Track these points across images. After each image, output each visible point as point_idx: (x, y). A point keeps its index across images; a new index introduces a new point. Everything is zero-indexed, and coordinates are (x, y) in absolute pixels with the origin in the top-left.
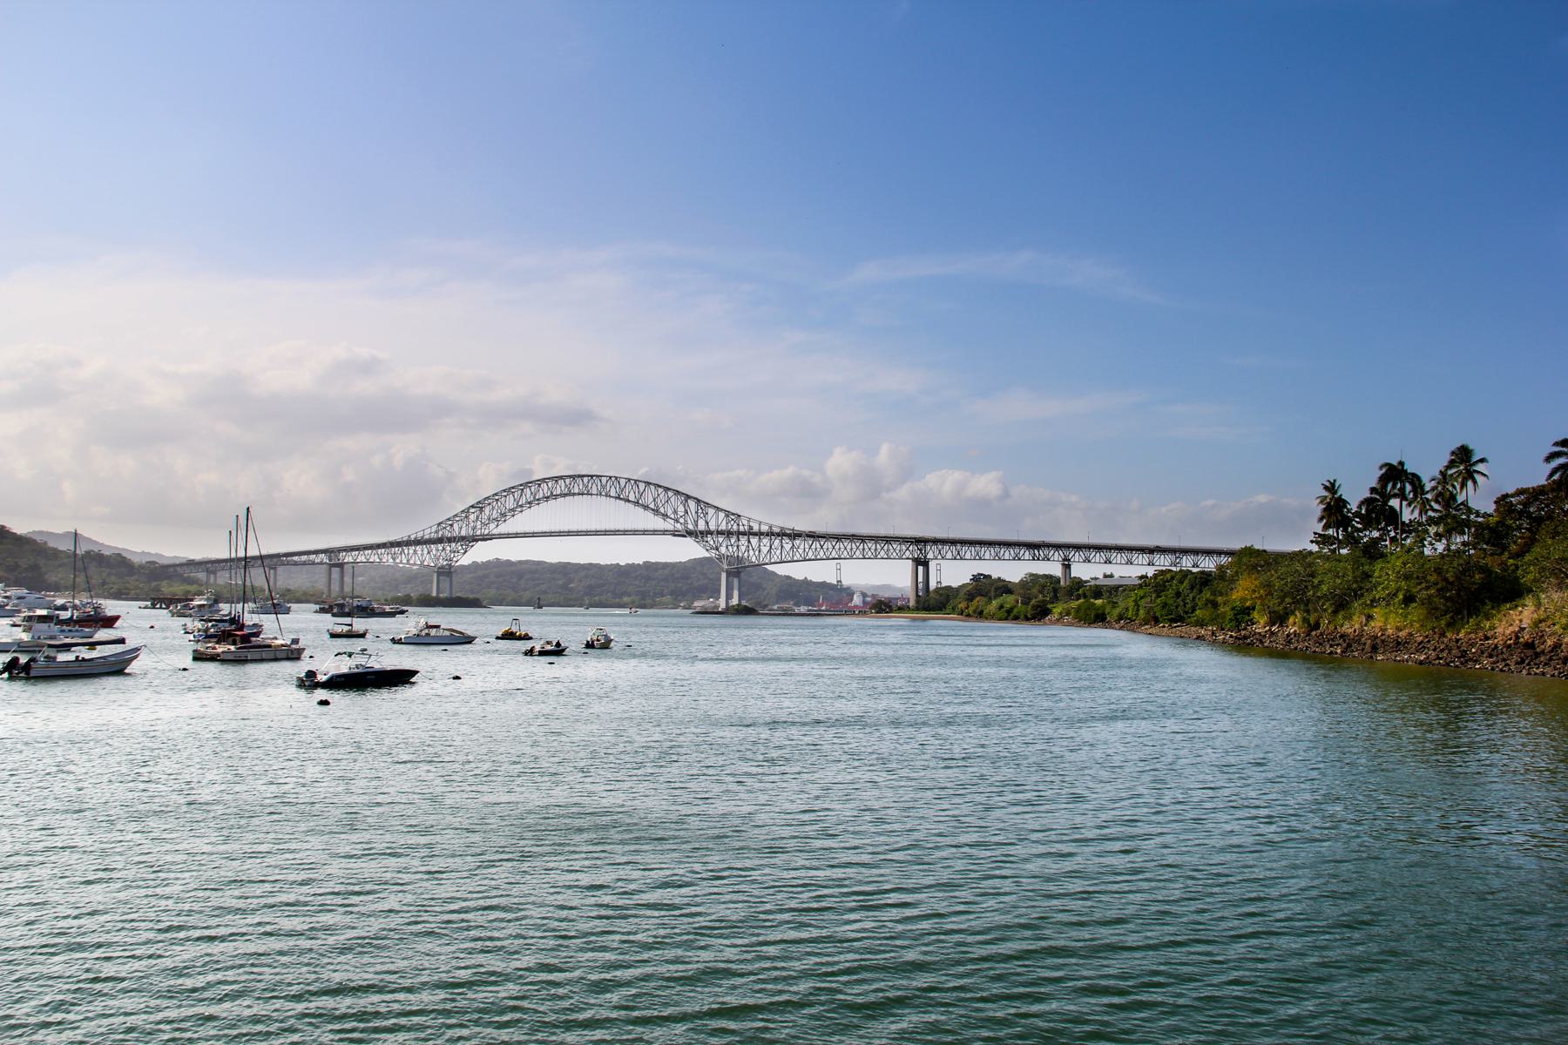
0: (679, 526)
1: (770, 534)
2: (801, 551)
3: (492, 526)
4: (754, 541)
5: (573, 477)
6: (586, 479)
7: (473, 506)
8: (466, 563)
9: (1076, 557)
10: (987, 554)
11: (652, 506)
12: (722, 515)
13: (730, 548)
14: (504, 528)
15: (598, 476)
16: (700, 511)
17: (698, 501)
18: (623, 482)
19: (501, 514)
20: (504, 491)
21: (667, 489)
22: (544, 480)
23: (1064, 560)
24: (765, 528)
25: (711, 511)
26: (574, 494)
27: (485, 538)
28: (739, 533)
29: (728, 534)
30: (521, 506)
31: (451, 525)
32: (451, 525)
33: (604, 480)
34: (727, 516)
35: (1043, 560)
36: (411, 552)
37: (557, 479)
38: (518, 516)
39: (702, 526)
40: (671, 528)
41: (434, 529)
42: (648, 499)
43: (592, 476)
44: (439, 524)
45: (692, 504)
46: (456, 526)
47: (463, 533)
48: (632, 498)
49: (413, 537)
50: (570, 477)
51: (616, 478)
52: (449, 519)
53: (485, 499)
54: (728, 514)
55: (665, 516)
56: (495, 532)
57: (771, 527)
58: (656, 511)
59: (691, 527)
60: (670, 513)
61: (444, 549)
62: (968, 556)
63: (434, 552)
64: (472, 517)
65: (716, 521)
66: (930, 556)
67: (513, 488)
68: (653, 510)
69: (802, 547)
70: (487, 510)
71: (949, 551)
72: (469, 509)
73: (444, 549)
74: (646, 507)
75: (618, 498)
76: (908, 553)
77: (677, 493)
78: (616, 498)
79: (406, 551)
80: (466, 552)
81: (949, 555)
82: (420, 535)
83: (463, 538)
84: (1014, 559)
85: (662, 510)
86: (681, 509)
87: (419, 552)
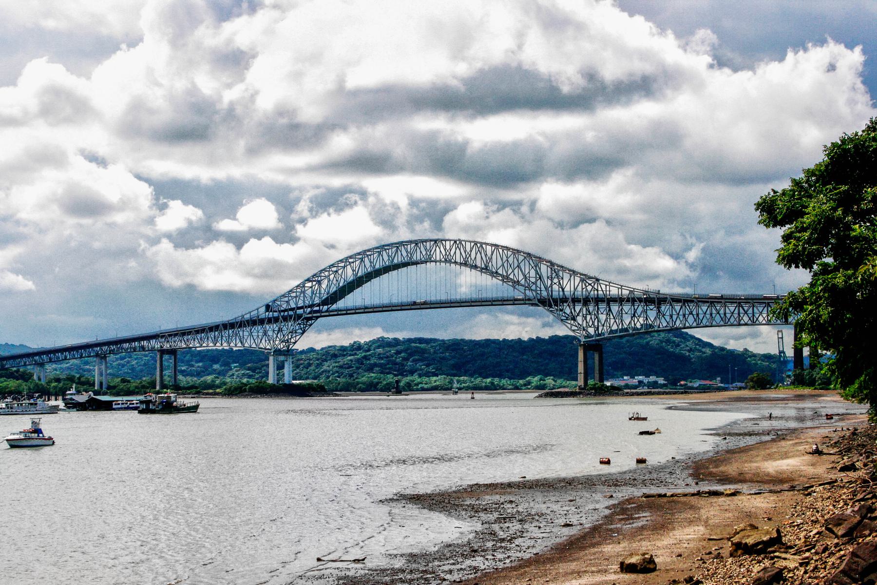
2: (668, 318)
7: (308, 280)
12: (577, 280)
13: (588, 317)
16: (554, 275)
24: (626, 292)
28: (598, 300)
29: (586, 301)
34: (582, 280)
36: (246, 333)
43: (436, 241)
49: (247, 317)
53: (321, 271)
54: (585, 278)
61: (280, 330)
65: (570, 286)
69: (668, 314)
72: (303, 284)
78: (461, 264)
79: (241, 333)
80: (304, 332)
86: (533, 273)
87: (255, 334)
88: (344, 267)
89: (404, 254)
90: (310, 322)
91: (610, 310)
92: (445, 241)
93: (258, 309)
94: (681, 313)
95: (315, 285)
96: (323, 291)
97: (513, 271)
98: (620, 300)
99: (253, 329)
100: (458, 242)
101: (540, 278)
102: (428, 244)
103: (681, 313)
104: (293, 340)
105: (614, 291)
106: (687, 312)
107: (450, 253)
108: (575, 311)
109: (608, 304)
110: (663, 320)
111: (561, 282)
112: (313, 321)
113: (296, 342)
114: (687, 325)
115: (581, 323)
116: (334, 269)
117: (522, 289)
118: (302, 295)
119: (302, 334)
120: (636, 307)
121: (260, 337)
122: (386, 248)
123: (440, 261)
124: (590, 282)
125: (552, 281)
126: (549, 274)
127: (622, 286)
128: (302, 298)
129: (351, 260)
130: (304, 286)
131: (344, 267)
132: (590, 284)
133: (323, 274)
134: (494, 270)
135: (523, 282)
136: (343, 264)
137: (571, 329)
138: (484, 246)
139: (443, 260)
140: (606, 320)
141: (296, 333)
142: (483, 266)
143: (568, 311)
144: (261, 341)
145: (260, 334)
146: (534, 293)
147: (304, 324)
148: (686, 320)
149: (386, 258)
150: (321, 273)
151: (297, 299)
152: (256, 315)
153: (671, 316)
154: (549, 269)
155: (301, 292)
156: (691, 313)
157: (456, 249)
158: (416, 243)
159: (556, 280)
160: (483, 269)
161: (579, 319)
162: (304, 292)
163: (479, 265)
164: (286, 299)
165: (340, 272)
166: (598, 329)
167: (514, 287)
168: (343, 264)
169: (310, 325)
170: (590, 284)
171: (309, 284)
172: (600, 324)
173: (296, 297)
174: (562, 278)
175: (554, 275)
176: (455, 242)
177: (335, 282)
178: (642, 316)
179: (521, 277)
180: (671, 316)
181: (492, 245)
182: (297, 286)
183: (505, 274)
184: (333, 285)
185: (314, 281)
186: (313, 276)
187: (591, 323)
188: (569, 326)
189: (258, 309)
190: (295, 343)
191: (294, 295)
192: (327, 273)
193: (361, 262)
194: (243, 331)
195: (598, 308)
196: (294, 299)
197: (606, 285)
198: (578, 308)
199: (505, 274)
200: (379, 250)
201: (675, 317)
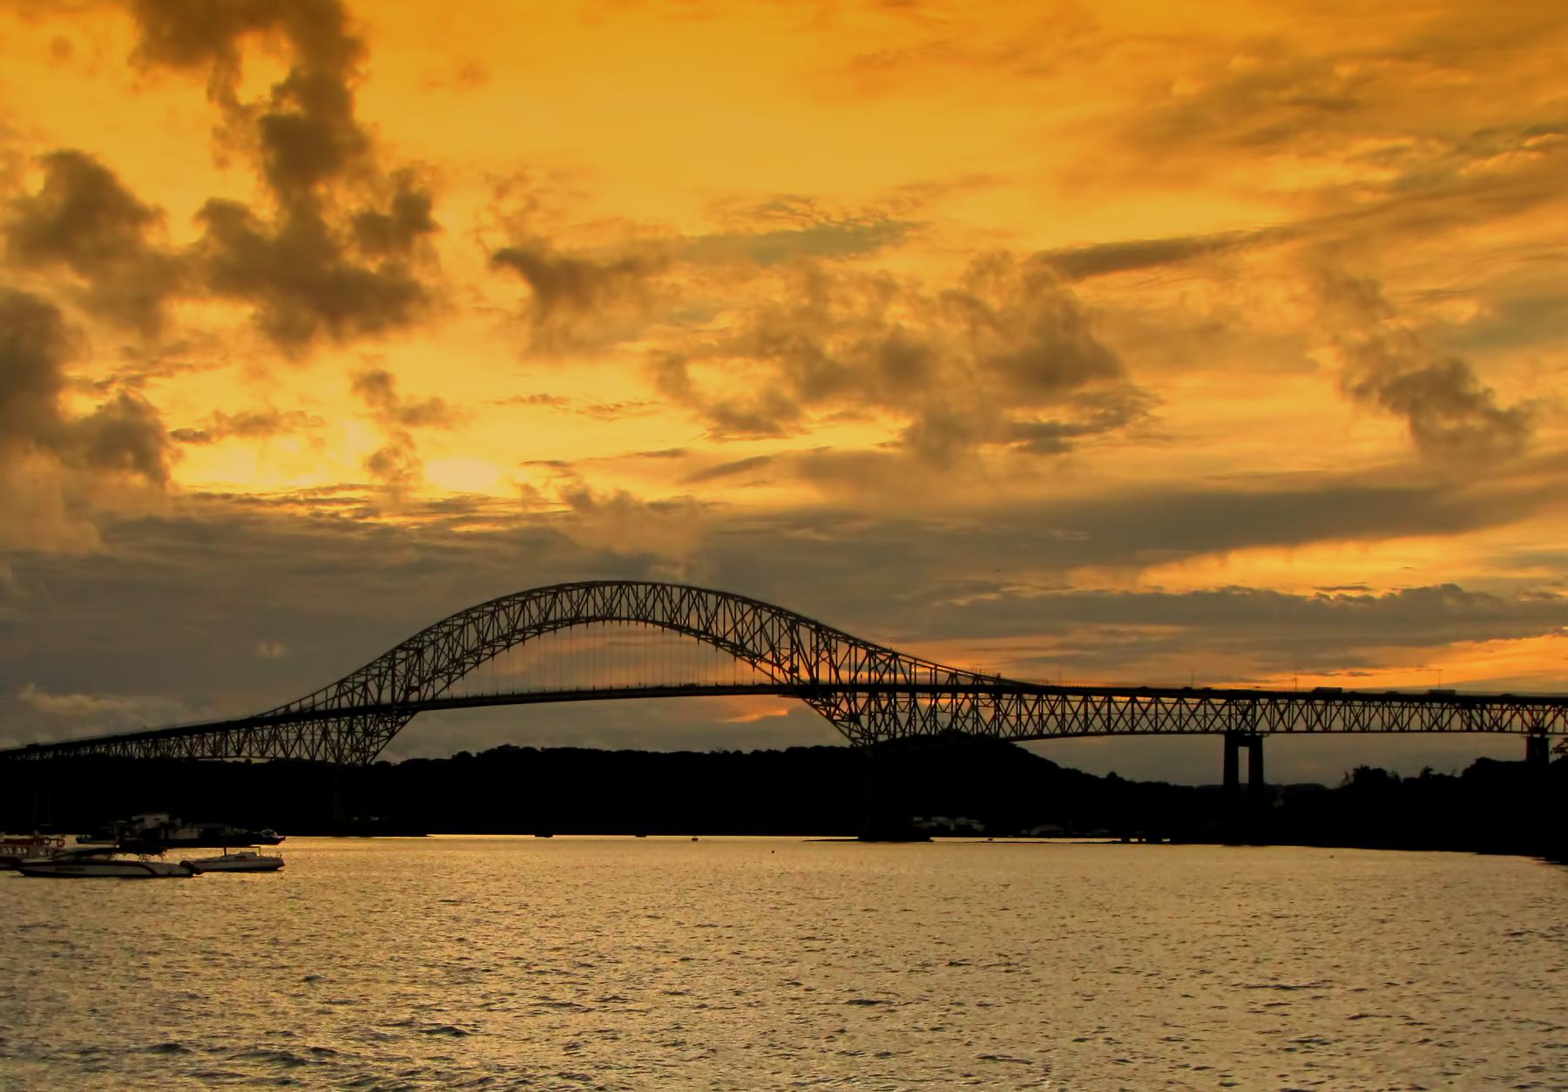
0: (780, 676)
1: (953, 688)
2: (1013, 721)
3: (440, 683)
4: (924, 702)
7: (401, 647)
8: (396, 760)
10: (1416, 718)
11: (730, 638)
12: (862, 653)
13: (879, 716)
14: (459, 689)
15: (629, 584)
16: (821, 646)
17: (819, 629)
18: (676, 593)
19: (453, 660)
20: (458, 615)
21: (757, 606)
22: (529, 595)
23: (1532, 730)
24: (943, 678)
25: (843, 648)
26: (588, 620)
27: (436, 704)
28: (893, 689)
29: (873, 689)
30: (491, 644)
32: (365, 685)
34: (870, 654)
35: (1490, 730)
36: (293, 736)
38: (487, 665)
39: (824, 675)
40: (767, 680)
41: (332, 692)
42: (724, 625)
43: (620, 584)
44: (341, 683)
45: (805, 634)
46: (372, 686)
47: (386, 697)
48: (693, 622)
49: (295, 708)
51: (663, 586)
52: (358, 673)
53: (423, 633)
54: (873, 651)
55: (754, 657)
56: (445, 694)
58: (738, 650)
61: (351, 731)
62: (1338, 724)
63: (334, 736)
64: (401, 668)
66: (1263, 725)
67: (474, 609)
68: (733, 646)
69: (1014, 713)
70: (429, 654)
71: (1300, 716)
72: (393, 652)
73: (351, 731)
74: (717, 641)
77: (779, 612)
78: (662, 624)
79: (284, 735)
80: (392, 734)
81: (1300, 725)
82: (307, 702)
83: (379, 710)
84: (1430, 730)
85: (749, 646)
86: (786, 642)
87: (308, 738)
88: (462, 627)
89: (567, 605)
90: (403, 718)
91: (916, 705)
92: (637, 584)
93: (313, 695)
94: (1036, 712)
95: (413, 656)
96: (426, 668)
97: (752, 638)
98: (934, 689)
99: (305, 728)
100: (659, 588)
101: (798, 650)
102: (608, 589)
103: (1036, 712)
104: (372, 749)
105: (922, 674)
106: (1046, 711)
107: (645, 605)
108: (856, 704)
109: (913, 696)
110: (1005, 724)
111: (834, 656)
113: (378, 751)
114: (1046, 731)
115: (866, 727)
116: (446, 629)
117: (767, 667)
118: (390, 672)
119: (389, 738)
120: (960, 701)
121: (317, 742)
122: (535, 594)
123: (628, 619)
124: (883, 658)
125: (818, 656)
126: (814, 643)
127: (936, 665)
128: (389, 678)
129: (475, 615)
130: (393, 658)
131: (462, 627)
133: (426, 638)
134: (719, 636)
135: (769, 657)
136: (460, 622)
137: (849, 737)
138: (703, 594)
139: (633, 617)
140: (909, 722)
141: (378, 736)
142: (702, 629)
143: (844, 707)
144: (318, 750)
145: (317, 738)
146: (789, 676)
147: (392, 722)
148: (1045, 724)
149: (535, 611)
151: (382, 679)
152: (311, 705)
153: (1019, 716)
154: (814, 636)
155: (389, 668)
156: (1052, 712)
157: (655, 601)
158: (589, 587)
159: (825, 655)
160: (701, 633)
161: (864, 720)
162: (392, 667)
163: (695, 627)
164: (363, 679)
165: (456, 634)
166: (895, 735)
167: (754, 665)
168: (460, 622)
171: (402, 655)
172: (898, 729)
173: (379, 676)
174: (836, 651)
175: (821, 646)
176: (654, 586)
177: (446, 650)
178: (971, 715)
179: (766, 647)
180: (1019, 716)
181: (717, 593)
182: (382, 658)
183: (738, 642)
184: (443, 657)
185: (412, 649)
186: (411, 640)
187: (883, 728)
188: (847, 731)
189: (313, 695)
190: (375, 754)
191: (376, 672)
192: (432, 637)
193: (492, 619)
194: (288, 732)
195: (896, 702)
196: (377, 680)
197: (911, 664)
198: (861, 702)
199: (738, 642)
200: (523, 598)
201: (1024, 719)
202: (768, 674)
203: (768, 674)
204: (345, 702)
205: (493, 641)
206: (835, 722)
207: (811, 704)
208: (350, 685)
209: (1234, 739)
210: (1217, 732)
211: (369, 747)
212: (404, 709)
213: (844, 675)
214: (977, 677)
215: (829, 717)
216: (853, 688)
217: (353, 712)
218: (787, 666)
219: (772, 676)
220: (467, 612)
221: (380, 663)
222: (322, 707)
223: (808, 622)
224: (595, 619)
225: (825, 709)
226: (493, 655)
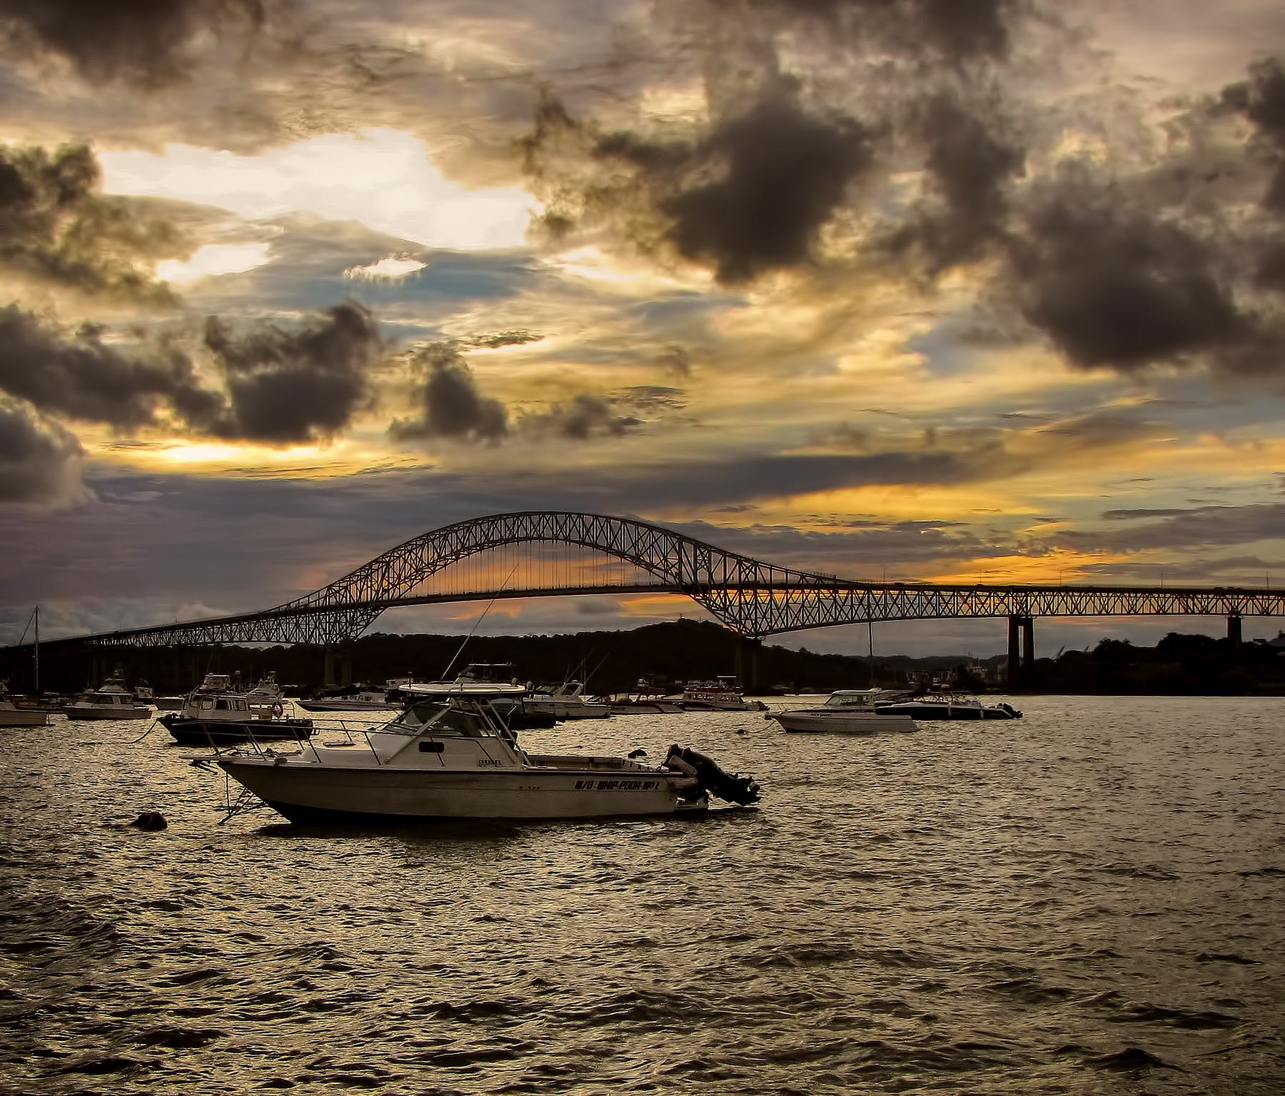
0: (670, 578)
5: (517, 516)
6: (535, 519)
7: (376, 561)
9: (1248, 607)
11: (632, 552)
14: (421, 589)
15: (552, 513)
20: (420, 538)
24: (793, 578)
25: (716, 557)
26: (519, 540)
28: (755, 586)
31: (346, 588)
33: (561, 518)
37: (493, 519)
39: (703, 577)
42: (625, 544)
43: (544, 514)
44: (329, 587)
45: (689, 547)
47: (364, 598)
50: (513, 515)
51: (579, 515)
52: (343, 580)
53: (393, 551)
54: (740, 560)
56: (408, 595)
57: (803, 577)
58: (636, 560)
59: (687, 579)
60: (656, 560)
68: (631, 557)
72: (370, 564)
74: (621, 554)
75: (582, 542)
76: (1002, 607)
93: (308, 596)
105: (779, 577)
112: (380, 611)
130: (371, 568)
132: (747, 568)
150: (393, 552)
167: (650, 571)
169: (376, 616)
170: (747, 568)
176: (570, 514)
185: (384, 562)
186: (383, 556)
202: (662, 578)
203: (662, 578)
204: (333, 600)
205: (446, 556)
206: (713, 612)
207: (694, 598)
208: (337, 589)
209: (1015, 620)
210: (1006, 616)
211: (350, 633)
212: (378, 605)
213: (718, 577)
214: (819, 578)
215: (709, 608)
216: (725, 586)
217: (339, 608)
218: (674, 571)
219: (664, 579)
220: (428, 535)
221: (360, 572)
222: (312, 605)
223: (689, 540)
224: (527, 538)
225: (706, 603)
226: (445, 565)
